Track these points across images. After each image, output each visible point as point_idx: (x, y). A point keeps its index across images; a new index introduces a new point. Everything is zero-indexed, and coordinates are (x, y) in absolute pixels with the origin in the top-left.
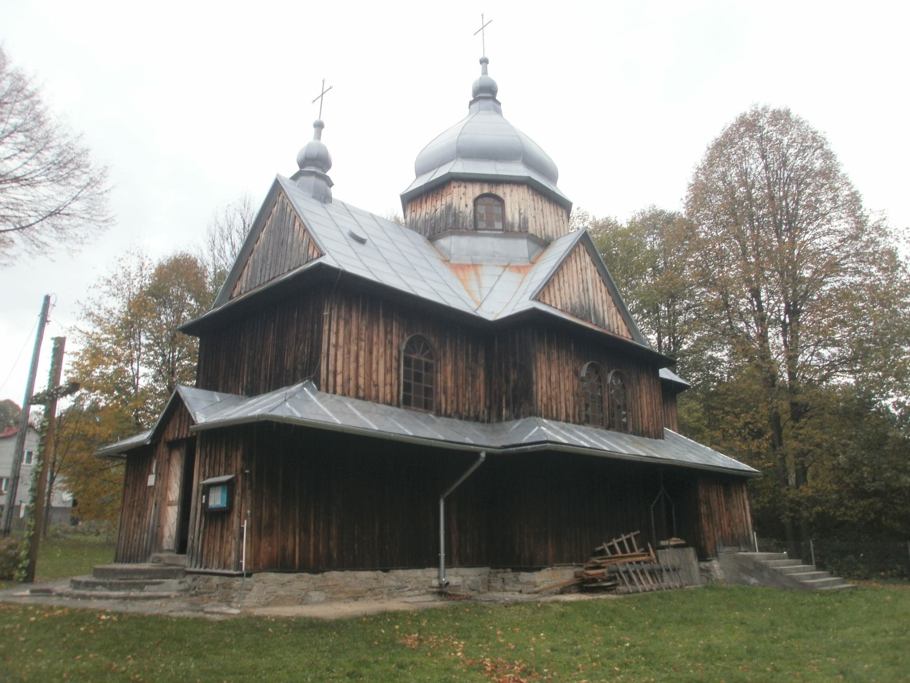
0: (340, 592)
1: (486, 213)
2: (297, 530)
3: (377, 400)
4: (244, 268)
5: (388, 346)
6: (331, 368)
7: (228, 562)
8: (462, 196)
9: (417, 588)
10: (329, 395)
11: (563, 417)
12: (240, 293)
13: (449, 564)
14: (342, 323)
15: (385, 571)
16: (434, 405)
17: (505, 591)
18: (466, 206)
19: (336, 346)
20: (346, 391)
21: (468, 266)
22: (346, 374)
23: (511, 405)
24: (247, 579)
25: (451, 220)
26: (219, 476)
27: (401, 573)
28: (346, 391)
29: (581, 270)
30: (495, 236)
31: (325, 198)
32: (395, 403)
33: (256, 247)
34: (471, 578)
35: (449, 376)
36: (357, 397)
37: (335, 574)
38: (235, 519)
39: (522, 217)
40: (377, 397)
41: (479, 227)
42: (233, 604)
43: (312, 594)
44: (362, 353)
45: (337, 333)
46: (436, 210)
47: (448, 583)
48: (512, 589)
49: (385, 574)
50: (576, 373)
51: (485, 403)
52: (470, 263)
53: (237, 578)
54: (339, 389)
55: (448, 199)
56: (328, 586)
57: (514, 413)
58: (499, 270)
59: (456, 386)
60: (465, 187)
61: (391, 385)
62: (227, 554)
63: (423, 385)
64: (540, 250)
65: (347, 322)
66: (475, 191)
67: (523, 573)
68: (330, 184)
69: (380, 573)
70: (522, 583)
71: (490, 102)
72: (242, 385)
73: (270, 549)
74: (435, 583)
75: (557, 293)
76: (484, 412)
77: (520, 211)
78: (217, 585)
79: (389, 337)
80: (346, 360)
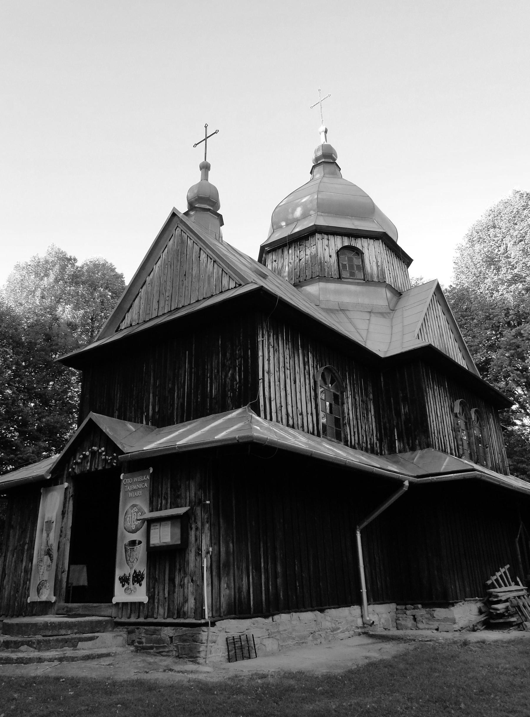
1: (348, 264)
2: (251, 568)
4: (134, 301)
5: (307, 376)
6: (267, 394)
7: (186, 609)
8: (326, 247)
9: (347, 630)
11: (449, 452)
12: (131, 325)
14: (271, 350)
15: (322, 611)
16: (342, 435)
17: (418, 628)
18: (330, 256)
19: (269, 372)
20: (279, 419)
21: (337, 310)
22: (278, 402)
23: (405, 439)
24: (212, 629)
25: (317, 268)
26: (161, 509)
27: (333, 613)
28: (279, 419)
29: (437, 317)
30: (358, 284)
31: (219, 238)
32: (316, 432)
33: (148, 279)
34: (384, 616)
35: (350, 409)
36: (288, 425)
37: (283, 617)
38: (192, 556)
39: (379, 269)
40: (303, 426)
41: (343, 276)
42: (201, 660)
44: (288, 381)
45: (269, 360)
46: (300, 260)
47: (373, 622)
48: (427, 626)
49: (322, 615)
50: (452, 410)
51: (376, 436)
52: (338, 308)
53: (204, 628)
55: (313, 250)
56: (279, 632)
57: (409, 445)
58: (367, 316)
59: (357, 419)
60: (328, 240)
61: (312, 414)
62: (181, 599)
64: (395, 299)
65: (276, 351)
66: (338, 243)
67: (438, 609)
68: (222, 224)
70: (438, 620)
71: (333, 167)
72: (147, 417)
73: (227, 591)
74: (360, 622)
76: (376, 445)
77: (377, 264)
78: (171, 638)
79: (307, 367)
80: (277, 388)
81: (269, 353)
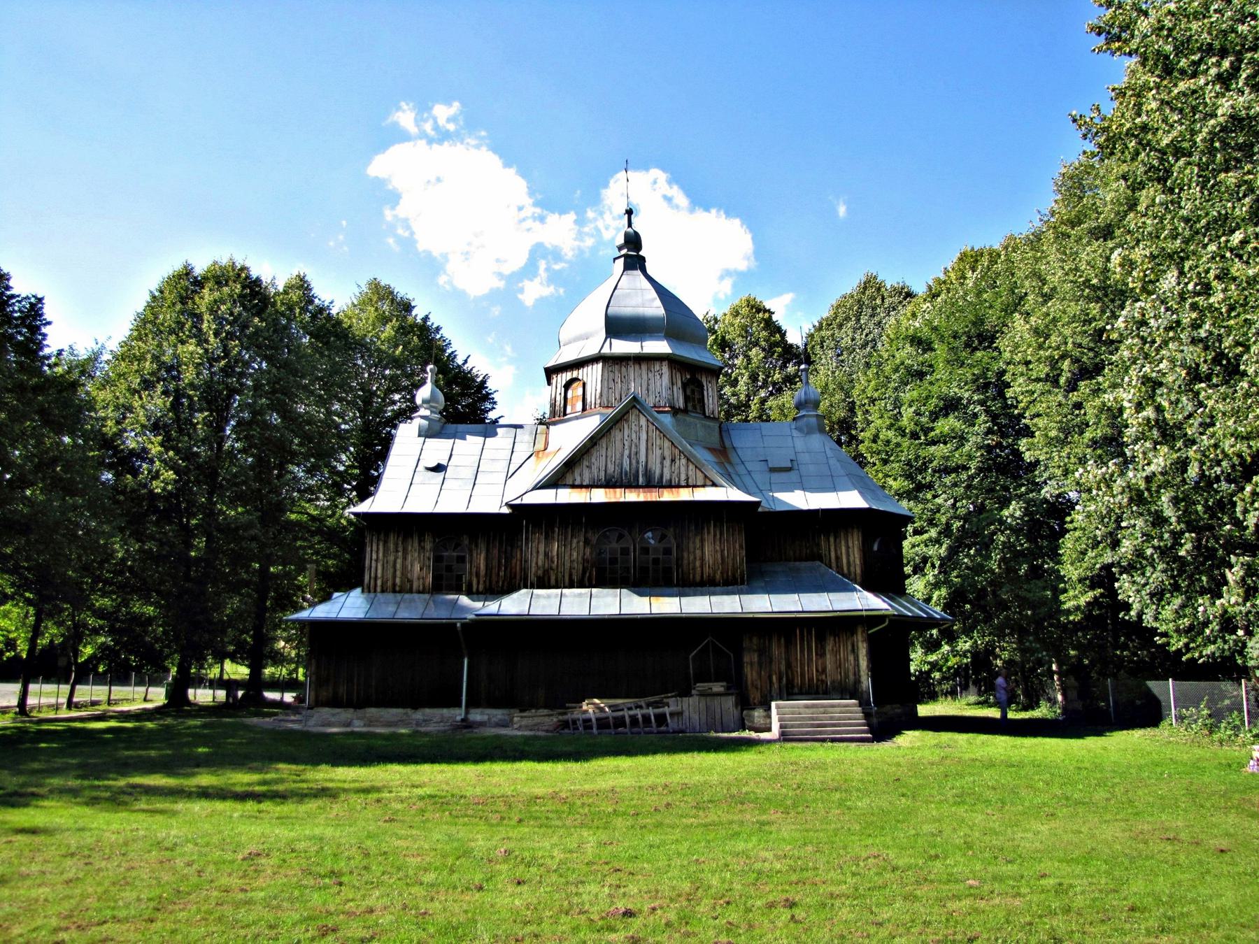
3: (411, 591)
6: (373, 575)
10: (372, 595)
27: (428, 711)
45: (377, 552)
54: (379, 589)
65: (386, 542)
69: (409, 711)
81: (378, 545)
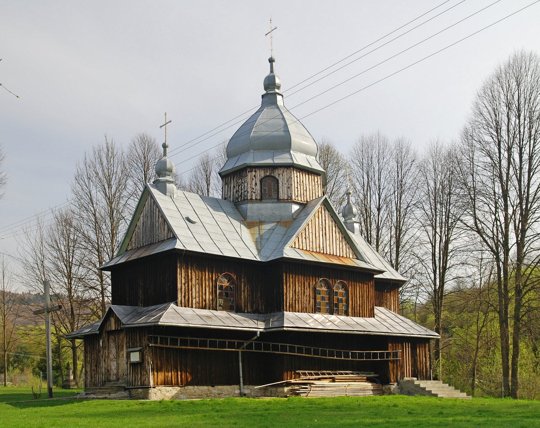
0: (193, 395)
2: (173, 369)
8: (254, 177)
9: (228, 394)
13: (244, 384)
27: (220, 387)
33: (139, 224)
43: (180, 395)
53: (150, 389)
60: (255, 172)
62: (144, 379)
63: (229, 298)
66: (260, 174)
75: (304, 240)
